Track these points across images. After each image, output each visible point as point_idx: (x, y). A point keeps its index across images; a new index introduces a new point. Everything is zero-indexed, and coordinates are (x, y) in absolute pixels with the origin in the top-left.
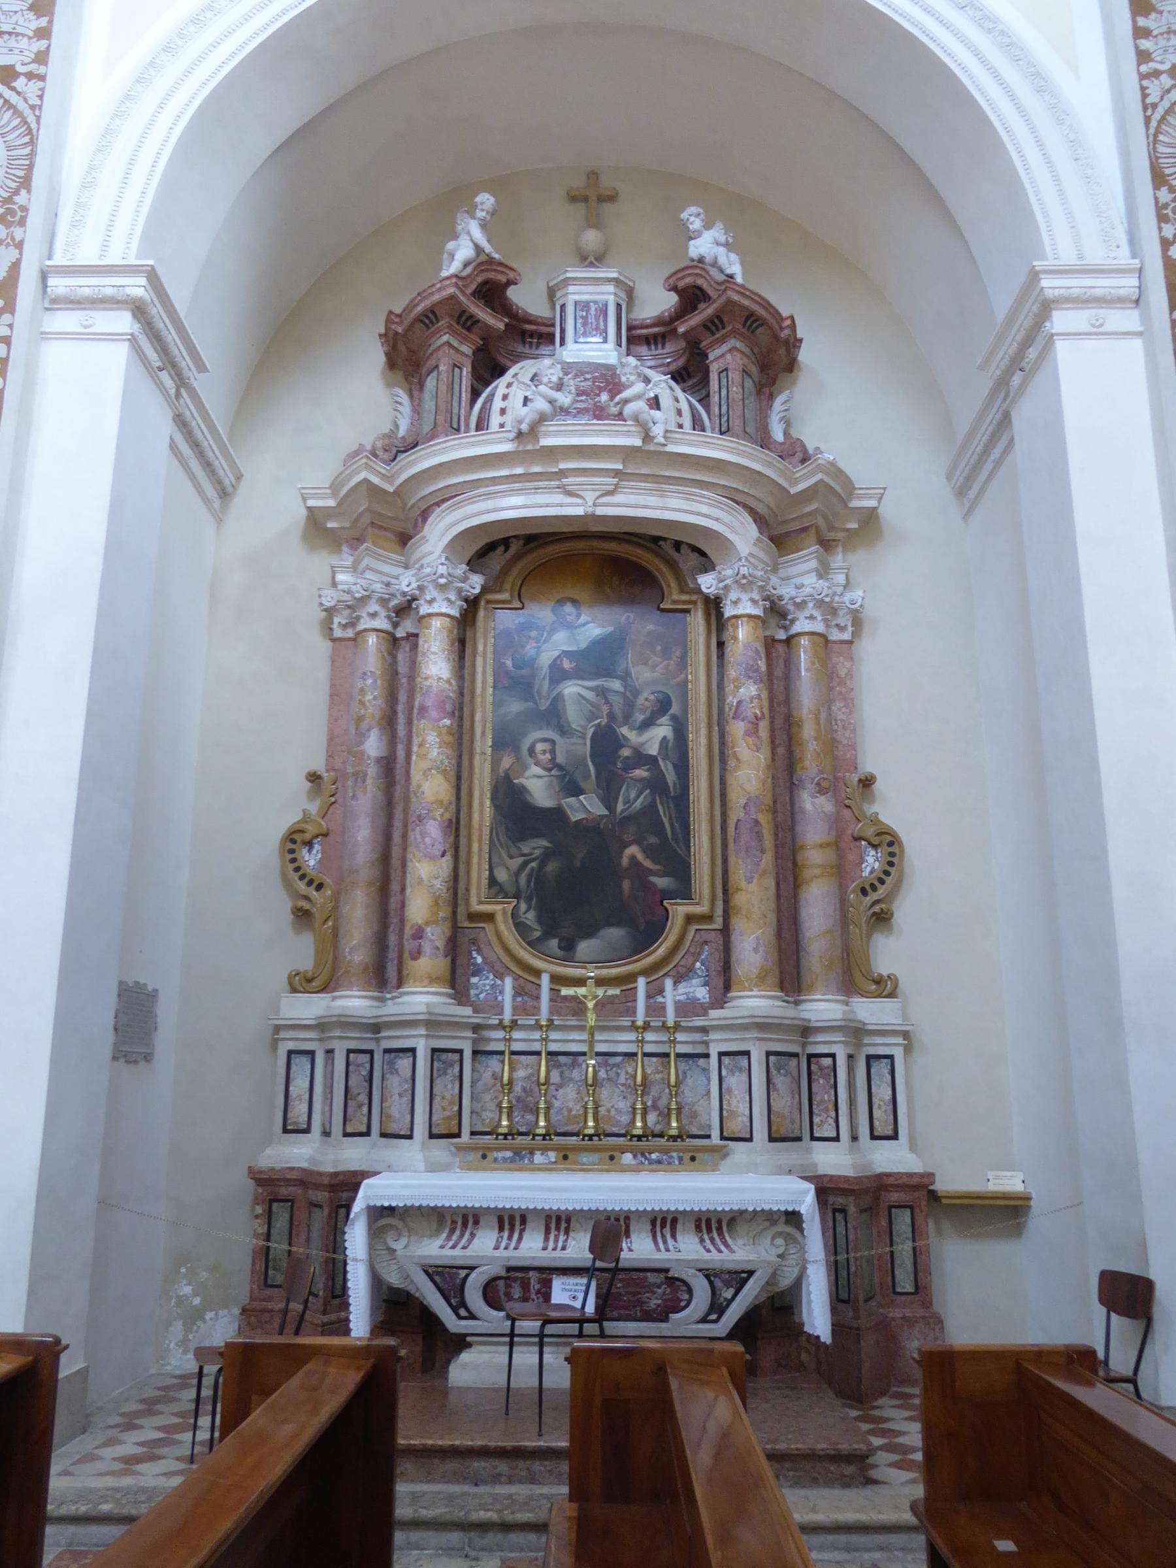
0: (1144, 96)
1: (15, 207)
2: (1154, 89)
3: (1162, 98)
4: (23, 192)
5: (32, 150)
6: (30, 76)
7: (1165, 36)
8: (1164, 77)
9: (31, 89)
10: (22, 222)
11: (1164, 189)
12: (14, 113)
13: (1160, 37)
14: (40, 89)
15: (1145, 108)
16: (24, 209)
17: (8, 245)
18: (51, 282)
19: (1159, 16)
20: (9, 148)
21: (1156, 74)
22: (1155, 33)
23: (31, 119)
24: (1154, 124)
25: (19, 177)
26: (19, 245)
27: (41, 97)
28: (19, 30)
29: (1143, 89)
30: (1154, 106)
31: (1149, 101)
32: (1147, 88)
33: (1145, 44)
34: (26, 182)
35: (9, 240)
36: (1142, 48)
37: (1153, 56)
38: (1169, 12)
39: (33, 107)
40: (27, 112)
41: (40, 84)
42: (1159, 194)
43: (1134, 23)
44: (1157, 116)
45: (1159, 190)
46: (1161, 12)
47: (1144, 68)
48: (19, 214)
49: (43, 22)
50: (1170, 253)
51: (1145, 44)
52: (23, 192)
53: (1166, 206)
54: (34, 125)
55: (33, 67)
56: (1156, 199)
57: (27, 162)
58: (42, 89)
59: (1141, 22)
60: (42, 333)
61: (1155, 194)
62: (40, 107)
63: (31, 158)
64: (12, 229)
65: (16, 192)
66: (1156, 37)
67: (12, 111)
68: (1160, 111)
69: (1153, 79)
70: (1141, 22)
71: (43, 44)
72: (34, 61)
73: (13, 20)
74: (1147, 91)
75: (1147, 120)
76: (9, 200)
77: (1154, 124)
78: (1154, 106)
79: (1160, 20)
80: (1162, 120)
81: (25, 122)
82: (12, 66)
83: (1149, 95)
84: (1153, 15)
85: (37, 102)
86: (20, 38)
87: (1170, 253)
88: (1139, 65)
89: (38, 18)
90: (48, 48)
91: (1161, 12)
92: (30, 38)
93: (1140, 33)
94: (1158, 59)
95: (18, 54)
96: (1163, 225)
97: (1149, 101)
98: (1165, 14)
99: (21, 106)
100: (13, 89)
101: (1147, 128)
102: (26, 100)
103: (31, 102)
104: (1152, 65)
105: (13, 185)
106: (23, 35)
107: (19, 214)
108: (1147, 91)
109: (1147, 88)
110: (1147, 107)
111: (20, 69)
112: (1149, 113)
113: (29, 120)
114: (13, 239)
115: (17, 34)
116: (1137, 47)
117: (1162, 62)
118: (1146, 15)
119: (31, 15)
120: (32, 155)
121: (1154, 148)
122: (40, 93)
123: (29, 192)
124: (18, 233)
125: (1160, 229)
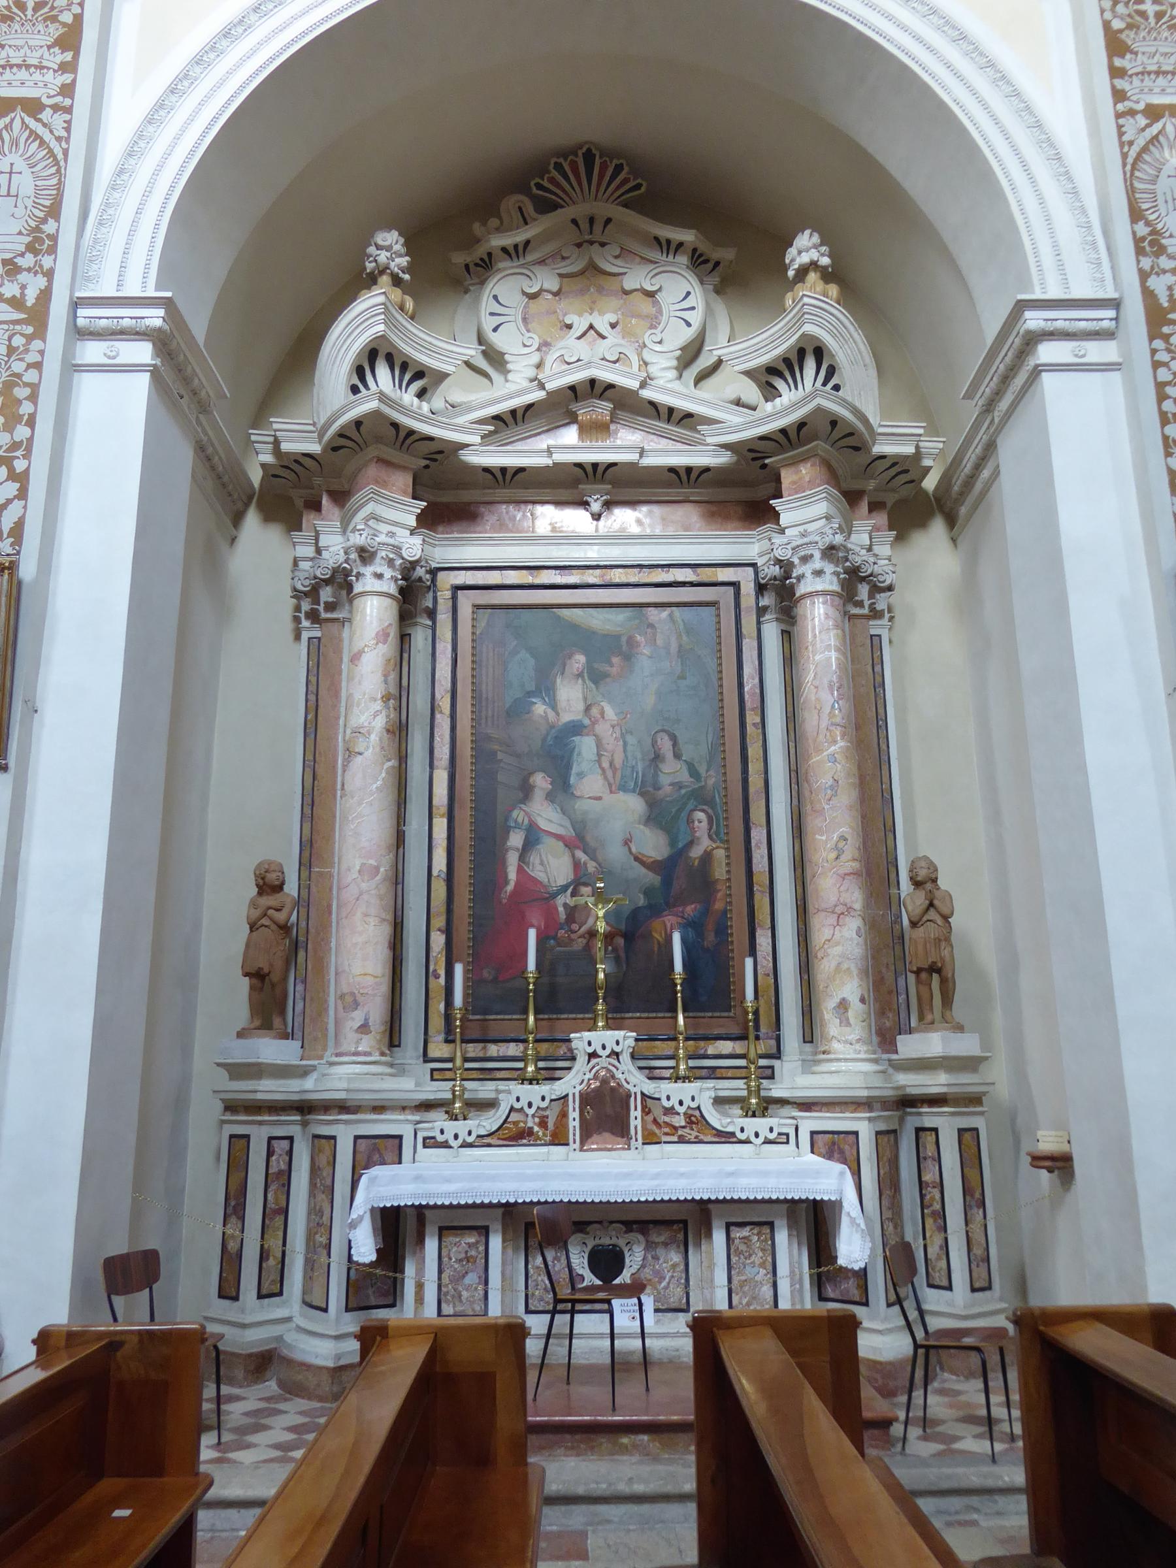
0: (1121, 134)
2: (1131, 126)
4: (51, 221)
5: (60, 179)
6: (56, 108)
7: (1140, 76)
8: (1139, 117)
9: (58, 121)
10: (52, 250)
11: (1141, 223)
12: (40, 145)
13: (1134, 77)
14: (64, 121)
15: (1122, 144)
16: (54, 238)
17: (36, 273)
18: (81, 312)
19: (1133, 56)
20: (37, 178)
21: (1132, 113)
23: (58, 151)
26: (49, 274)
27: (68, 129)
28: (45, 63)
29: (1119, 127)
30: (1131, 143)
31: (1125, 138)
32: (1123, 126)
33: (1120, 84)
34: (54, 211)
35: (37, 268)
36: (1119, 87)
37: (1129, 94)
38: (1144, 53)
39: (59, 139)
40: (53, 144)
41: (67, 117)
42: (1136, 227)
45: (1136, 223)
46: (1136, 53)
47: (1120, 107)
50: (1148, 284)
51: (1120, 84)
52: (51, 221)
53: (1143, 239)
54: (60, 156)
55: (59, 99)
56: (1134, 233)
57: (54, 192)
58: (69, 122)
59: (1118, 62)
60: (75, 366)
61: (1132, 228)
62: (68, 140)
63: (58, 189)
64: (40, 257)
65: (44, 221)
66: (1131, 76)
67: (37, 142)
69: (1129, 117)
70: (1118, 62)
71: (67, 78)
72: (58, 94)
73: (38, 54)
74: (1124, 129)
75: (1124, 156)
76: (37, 229)
77: (1130, 160)
78: (1131, 143)
79: (1135, 60)
80: (1138, 158)
81: (51, 152)
82: (39, 98)
83: (1125, 132)
84: (1128, 56)
86: (45, 71)
87: (1148, 284)
88: (1115, 105)
90: (74, 81)
91: (1136, 53)
92: (55, 71)
93: (1116, 73)
94: (1134, 98)
96: (1141, 258)
97: (1125, 138)
98: (1140, 56)
99: (47, 137)
100: (39, 120)
101: (1124, 165)
102: (51, 132)
103: (57, 134)
104: (1127, 103)
105: (41, 215)
106: (48, 68)
108: (1124, 129)
109: (1123, 126)
110: (1124, 145)
111: (45, 101)
112: (1126, 149)
113: (55, 151)
114: (41, 266)
115: (42, 68)
116: (1113, 87)
118: (1123, 56)
119: (56, 50)
120: (60, 188)
121: (1132, 185)
122: (65, 125)
123: (58, 220)
124: (47, 262)
125: (1138, 262)
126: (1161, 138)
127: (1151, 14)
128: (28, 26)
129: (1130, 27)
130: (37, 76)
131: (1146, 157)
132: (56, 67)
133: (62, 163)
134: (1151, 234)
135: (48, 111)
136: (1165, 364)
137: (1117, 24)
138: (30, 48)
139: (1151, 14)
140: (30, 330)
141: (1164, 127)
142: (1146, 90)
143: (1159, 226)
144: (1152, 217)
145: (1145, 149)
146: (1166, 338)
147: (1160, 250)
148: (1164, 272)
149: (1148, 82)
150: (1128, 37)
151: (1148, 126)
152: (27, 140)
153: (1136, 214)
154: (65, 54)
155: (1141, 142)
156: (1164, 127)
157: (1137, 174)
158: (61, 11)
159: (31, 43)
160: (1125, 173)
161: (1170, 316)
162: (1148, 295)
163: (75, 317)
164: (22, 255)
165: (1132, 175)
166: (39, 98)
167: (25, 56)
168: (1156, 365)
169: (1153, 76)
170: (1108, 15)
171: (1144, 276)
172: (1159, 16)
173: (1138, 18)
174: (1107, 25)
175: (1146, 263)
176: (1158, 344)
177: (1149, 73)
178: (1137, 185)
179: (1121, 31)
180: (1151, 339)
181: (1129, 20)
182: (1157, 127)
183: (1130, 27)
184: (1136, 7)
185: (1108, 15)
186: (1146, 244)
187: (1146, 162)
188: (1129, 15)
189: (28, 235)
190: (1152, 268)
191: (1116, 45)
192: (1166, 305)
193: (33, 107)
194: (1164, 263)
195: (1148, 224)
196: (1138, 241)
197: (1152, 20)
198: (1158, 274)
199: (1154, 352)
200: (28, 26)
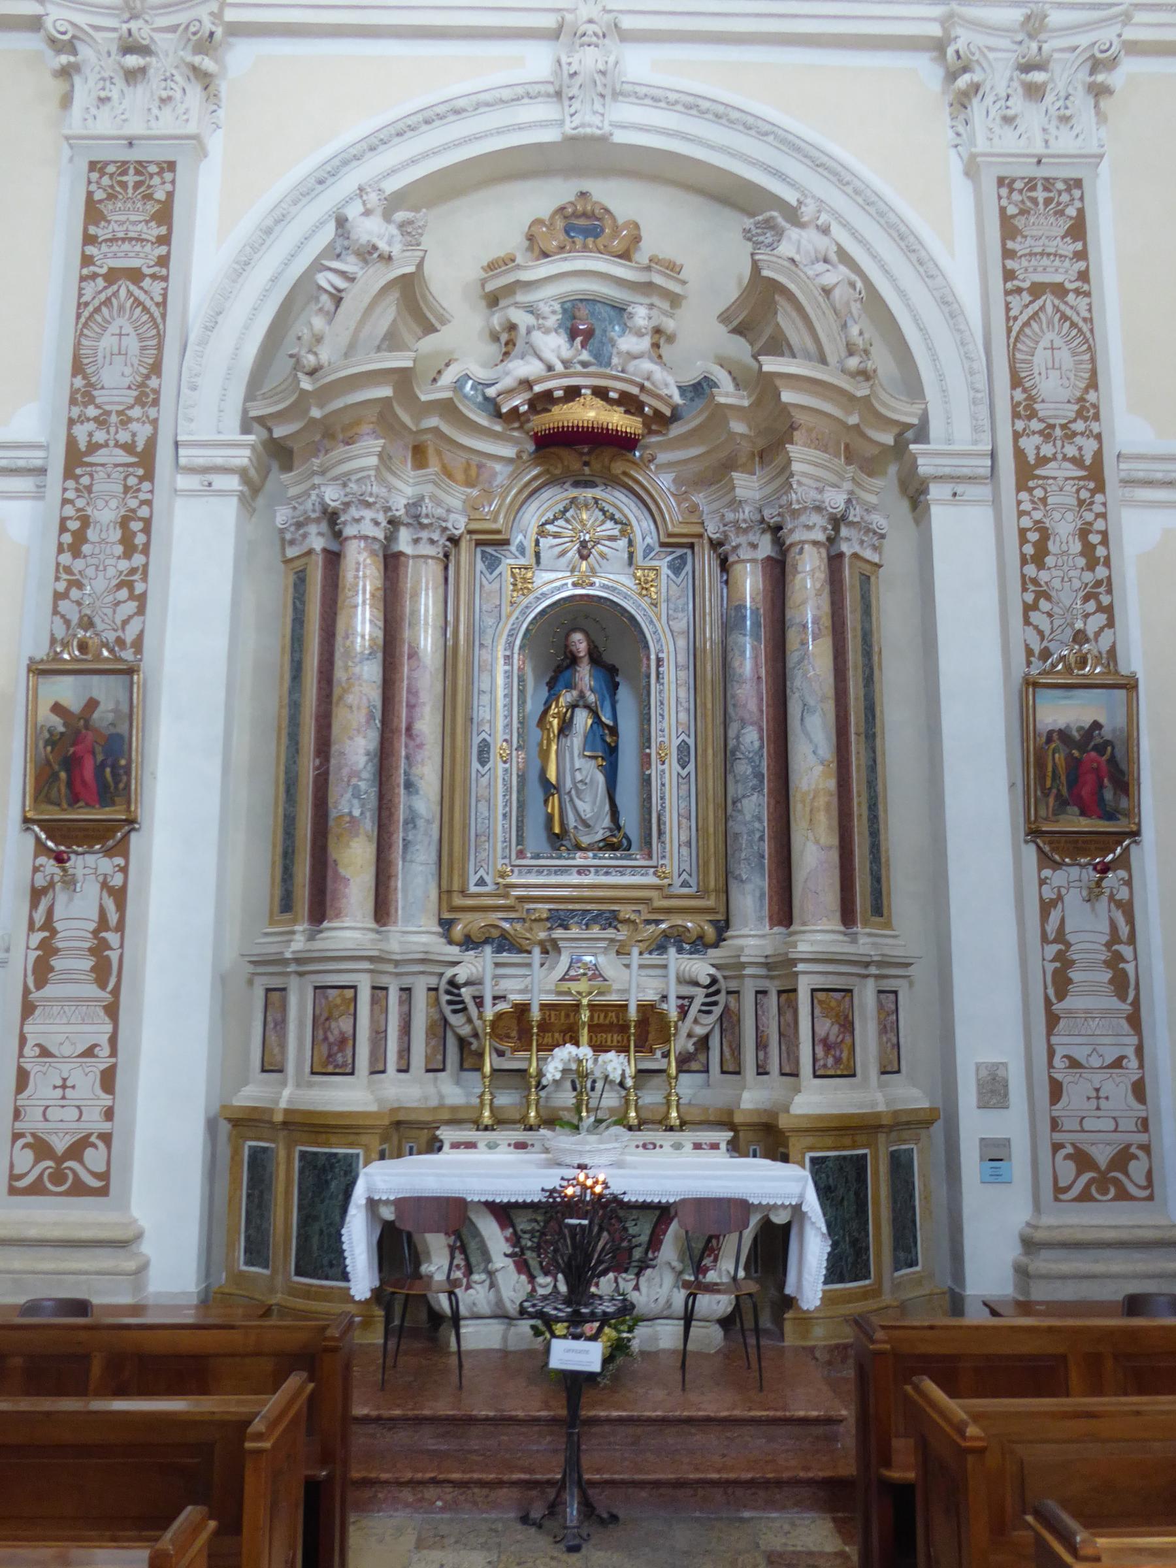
2: (1016, 302)
3: (1021, 313)
8: (1025, 294)
11: (1019, 390)
15: (1008, 319)
21: (1019, 291)
22: (1019, 254)
24: (1014, 334)
31: (1012, 313)
33: (1010, 264)
36: (1009, 267)
43: (1004, 245)
44: (1016, 328)
46: (1026, 237)
47: (1009, 285)
51: (1010, 264)
53: (1019, 404)
59: (1010, 245)
68: (1019, 323)
77: (1014, 334)
78: (1015, 319)
84: (1019, 239)
91: (1026, 237)
93: (1008, 254)
94: (1021, 277)
96: (1016, 421)
101: (1008, 337)
104: (1016, 283)
112: (1011, 323)
116: (1004, 266)
117: (1024, 280)
118: (1013, 239)
126: (1041, 315)
127: (1041, 200)
129: (1023, 212)
131: (1027, 331)
134: (1026, 400)
136: (1028, 513)
137: (1012, 210)
139: (1041, 200)
141: (1044, 305)
142: (1040, 269)
143: (1034, 393)
144: (1027, 385)
145: (1027, 324)
146: (1030, 490)
147: (1033, 415)
148: (1034, 433)
150: (1020, 222)
151: (1031, 302)
153: (1016, 381)
155: (1024, 317)
156: (1044, 305)
157: (1019, 346)
160: (1008, 345)
161: (1037, 472)
162: (1019, 454)
165: (1015, 345)
168: (1021, 514)
169: (1038, 257)
170: (1004, 202)
171: (1017, 436)
173: (1029, 204)
174: (1003, 210)
175: (1020, 425)
176: (1024, 496)
177: (1036, 254)
179: (1013, 216)
180: (1018, 490)
183: (1023, 212)
184: (1030, 194)
185: (1004, 202)
186: (1021, 408)
187: (1027, 336)
188: (1023, 202)
190: (1024, 430)
192: (1032, 462)
194: (1035, 425)
195: (1025, 390)
196: (1015, 406)
197: (1041, 206)
198: (1028, 435)
199: (1019, 503)
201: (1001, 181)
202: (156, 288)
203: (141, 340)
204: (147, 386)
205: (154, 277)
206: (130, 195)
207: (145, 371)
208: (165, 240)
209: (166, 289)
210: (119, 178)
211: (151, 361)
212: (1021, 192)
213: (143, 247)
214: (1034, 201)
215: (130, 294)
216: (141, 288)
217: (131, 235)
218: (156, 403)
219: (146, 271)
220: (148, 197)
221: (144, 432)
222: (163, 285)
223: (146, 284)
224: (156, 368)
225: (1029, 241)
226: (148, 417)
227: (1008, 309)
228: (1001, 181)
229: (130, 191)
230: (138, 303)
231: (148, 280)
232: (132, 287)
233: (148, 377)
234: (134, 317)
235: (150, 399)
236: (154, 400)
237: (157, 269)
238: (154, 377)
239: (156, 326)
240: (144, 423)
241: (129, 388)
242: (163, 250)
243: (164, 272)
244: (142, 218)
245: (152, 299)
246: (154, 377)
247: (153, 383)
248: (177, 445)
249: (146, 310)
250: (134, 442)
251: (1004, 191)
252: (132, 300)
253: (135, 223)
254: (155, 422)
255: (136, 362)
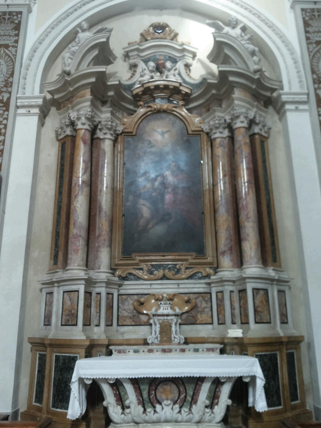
1: (9, 82)
2: (311, 47)
14: (15, 50)
16: (12, 83)
21: (311, 43)
25: (9, 74)
27: (16, 52)
30: (311, 52)
31: (310, 50)
33: (308, 35)
35: (7, 91)
39: (13, 55)
40: (12, 56)
44: (312, 54)
47: (308, 42)
48: (10, 84)
49: (17, 32)
51: (308, 35)
54: (14, 60)
59: (307, 29)
62: (16, 55)
70: (307, 29)
72: (14, 43)
75: (310, 55)
77: (311, 57)
80: (314, 56)
81: (11, 59)
82: (8, 44)
85: (15, 53)
89: (15, 31)
90: (18, 39)
91: (312, 27)
92: (13, 36)
93: (307, 32)
95: (10, 42)
97: (310, 50)
102: (12, 53)
104: (310, 41)
106: (11, 36)
107: (10, 84)
110: (309, 52)
117: (313, 40)
119: (13, 30)
120: (13, 68)
128: (6, 24)
129: (311, 19)
130: (8, 38)
132: (13, 35)
133: (14, 62)
135: (11, 48)
137: (307, 18)
138: (6, 30)
140: (4, 109)
145: (315, 53)
149: (316, 34)
150: (311, 22)
151: (316, 47)
152: (5, 55)
154: (16, 32)
155: (314, 51)
157: (314, 61)
158: (15, 20)
159: (7, 29)
163: (16, 102)
164: (3, 88)
166: (8, 44)
167: (5, 32)
170: (304, 16)
171: (315, 89)
172: (319, 16)
174: (304, 19)
178: (313, 64)
179: (307, 20)
181: (310, 17)
182: (318, 48)
183: (311, 19)
185: (304, 16)
188: (311, 16)
189: (4, 82)
191: (306, 24)
193: (7, 46)
195: (317, 74)
200: (6, 24)
201: (302, 10)
202: (13, 50)
203: (8, 66)
204: (8, 81)
205: (13, 46)
206: (6, 22)
207: (8, 76)
208: (17, 35)
209: (16, 50)
210: (3, 17)
211: (10, 73)
212: (309, 13)
213: (10, 37)
214: (314, 15)
215: (4, 52)
216: (8, 50)
217: (6, 34)
218: (11, 86)
219: (10, 44)
220: (13, 22)
221: (6, 96)
222: (16, 49)
223: (10, 49)
224: (12, 75)
225: (314, 28)
226: (8, 91)
227: (308, 48)
228: (302, 10)
229: (6, 20)
230: (7, 54)
231: (11, 48)
232: (5, 50)
233: (9, 78)
234: (5, 59)
235: (9, 85)
236: (10, 85)
237: (14, 44)
238: (11, 78)
239: (13, 61)
240: (7, 93)
241: (2, 82)
242: (16, 38)
243: (16, 45)
244: (10, 29)
245: (12, 53)
246: (11, 78)
247: (11, 80)
248: (17, 98)
249: (9, 57)
250: (3, 99)
251: (304, 13)
252: (5, 54)
253: (7, 30)
254: (10, 93)
255: (5, 74)
